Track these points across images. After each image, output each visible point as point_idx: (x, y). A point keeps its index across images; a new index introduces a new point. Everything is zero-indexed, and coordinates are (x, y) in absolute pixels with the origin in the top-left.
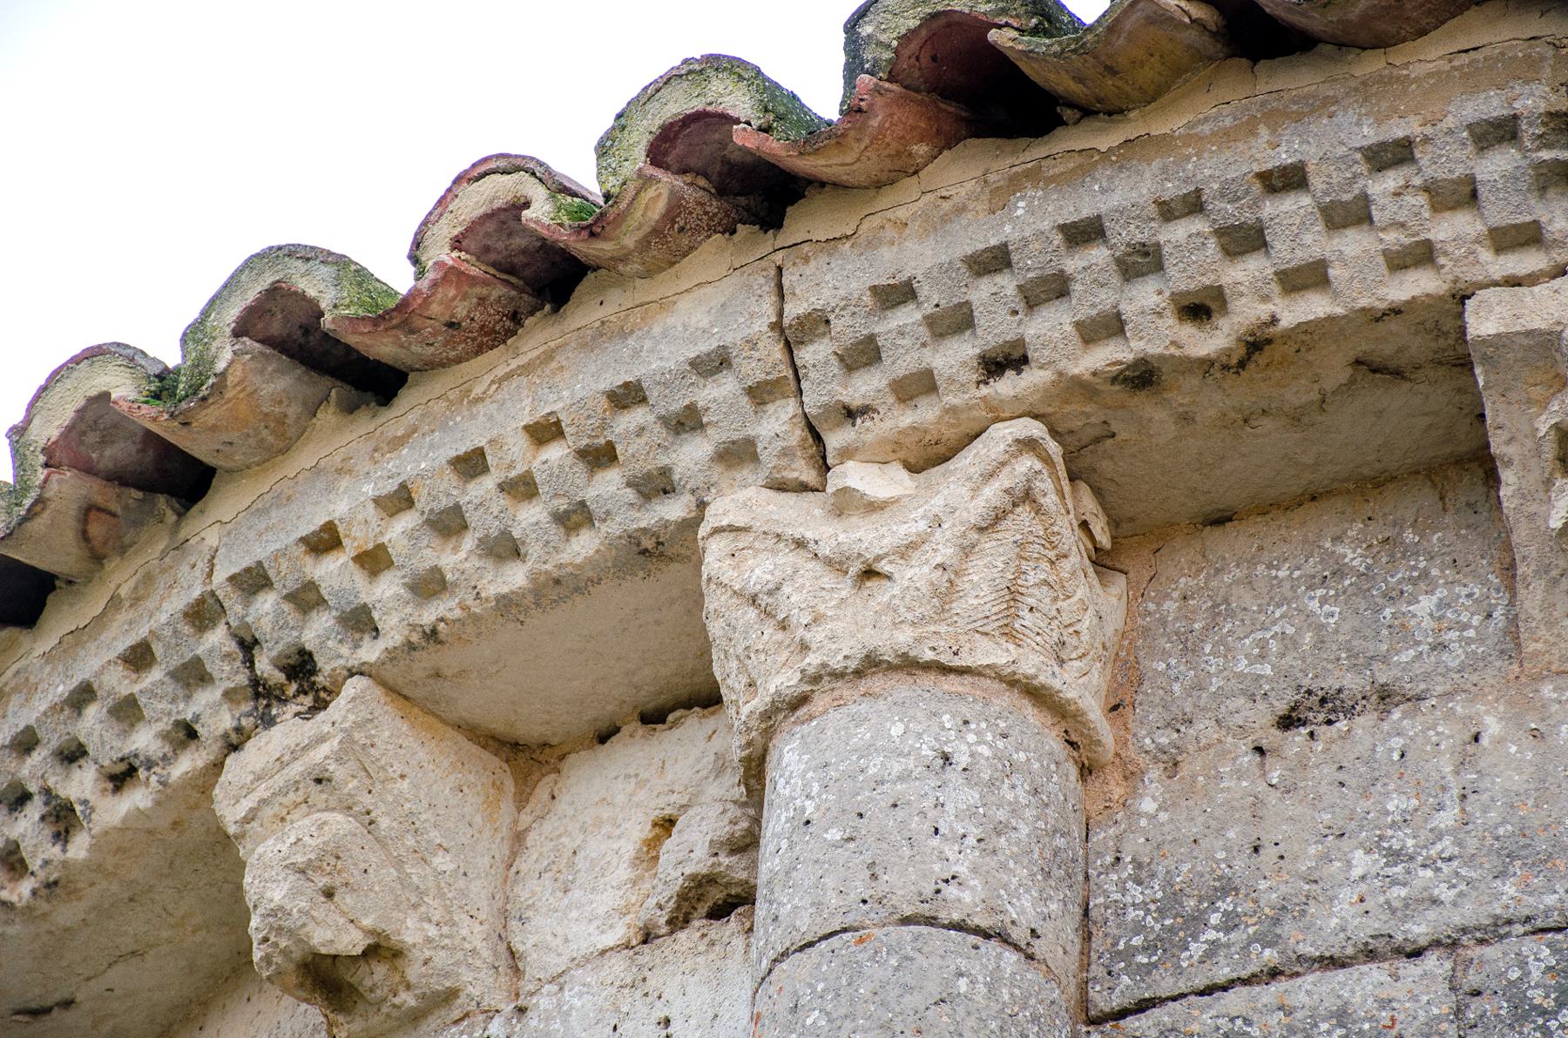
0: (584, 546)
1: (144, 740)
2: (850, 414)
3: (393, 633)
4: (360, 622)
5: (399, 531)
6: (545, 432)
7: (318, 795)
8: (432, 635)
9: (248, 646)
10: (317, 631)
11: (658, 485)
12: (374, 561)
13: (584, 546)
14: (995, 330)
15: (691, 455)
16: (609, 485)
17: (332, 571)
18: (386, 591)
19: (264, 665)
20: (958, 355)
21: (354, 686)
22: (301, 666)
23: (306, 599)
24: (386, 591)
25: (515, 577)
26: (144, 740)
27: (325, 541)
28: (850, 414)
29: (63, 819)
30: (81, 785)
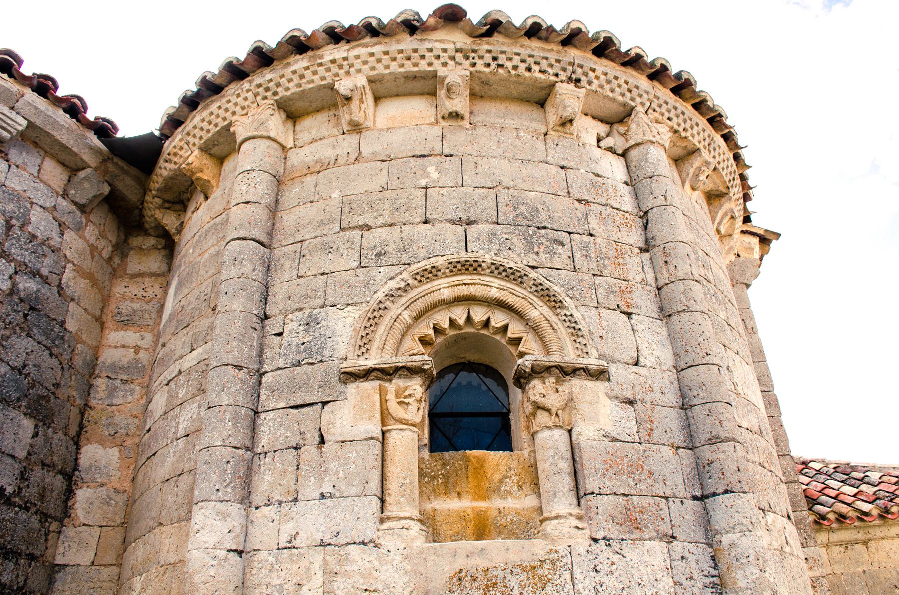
0: (620, 98)
1: (550, 71)
2: (654, 111)
3: (594, 87)
4: (590, 83)
5: (603, 77)
6: (627, 83)
7: (576, 99)
8: (596, 91)
9: (574, 72)
10: (583, 79)
11: (633, 99)
12: (597, 78)
13: (620, 98)
14: (672, 115)
15: (638, 100)
16: (628, 94)
17: (591, 74)
18: (596, 82)
19: (574, 76)
20: (667, 115)
21: (584, 89)
22: (578, 81)
23: (586, 74)
24: (596, 82)
25: (611, 95)
26: (550, 71)
27: (594, 70)
28: (654, 111)
29: (529, 69)
30: (536, 68)
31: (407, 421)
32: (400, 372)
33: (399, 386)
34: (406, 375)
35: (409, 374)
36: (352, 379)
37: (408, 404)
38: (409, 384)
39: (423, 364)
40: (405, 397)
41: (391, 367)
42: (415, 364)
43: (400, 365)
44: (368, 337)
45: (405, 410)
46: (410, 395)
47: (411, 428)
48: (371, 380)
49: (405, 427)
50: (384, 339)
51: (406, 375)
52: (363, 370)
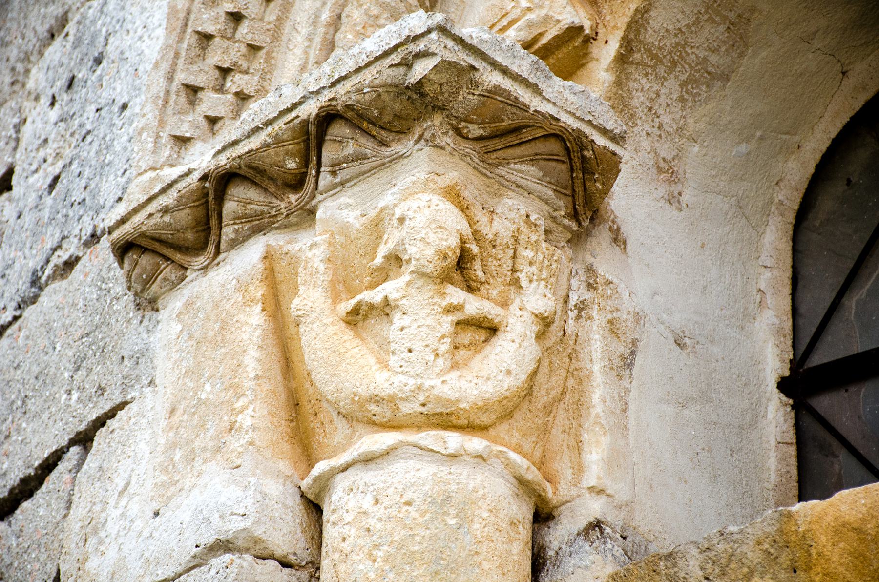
31: (391, 400)
32: (329, 153)
33: (344, 228)
34: (359, 158)
35: (367, 146)
36: (169, 272)
37: (386, 309)
38: (387, 199)
39: (407, 64)
40: (382, 275)
41: (278, 140)
42: (367, 76)
43: (310, 109)
44: (243, 28)
45: (384, 350)
46: (396, 259)
47: (429, 438)
48: (235, 244)
49: (388, 439)
50: (325, 16)
51: (359, 158)
52: (181, 203)
